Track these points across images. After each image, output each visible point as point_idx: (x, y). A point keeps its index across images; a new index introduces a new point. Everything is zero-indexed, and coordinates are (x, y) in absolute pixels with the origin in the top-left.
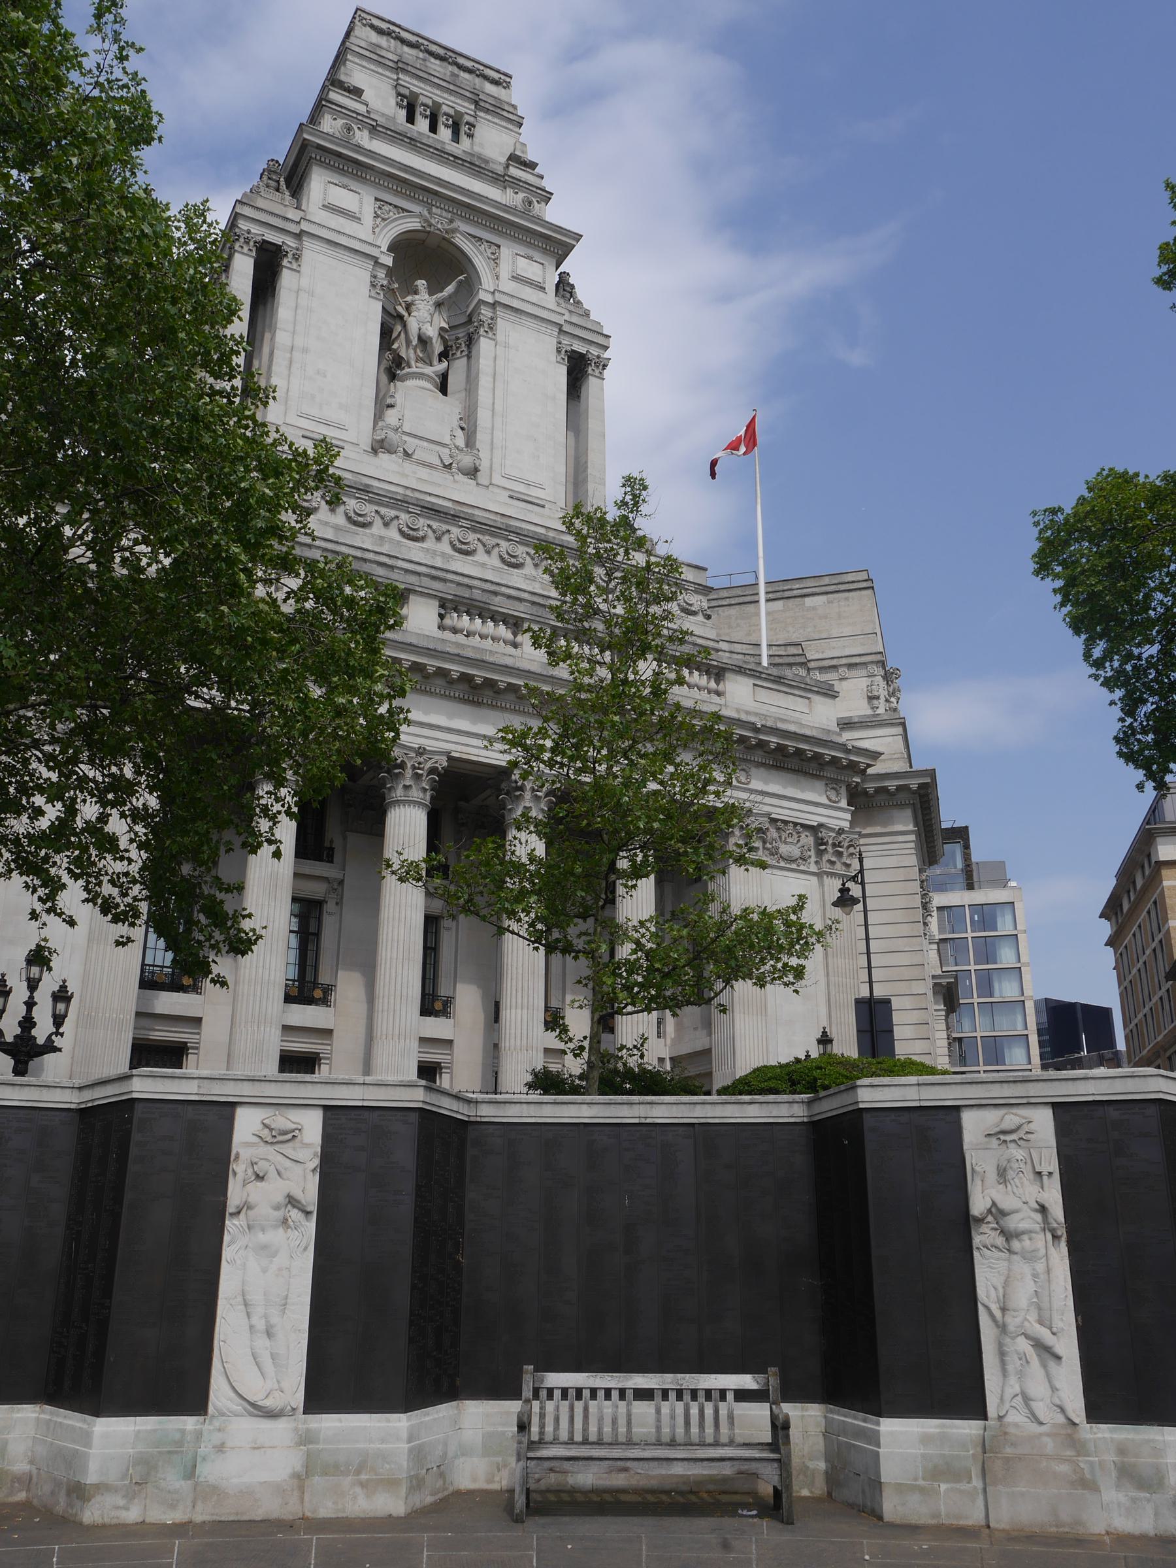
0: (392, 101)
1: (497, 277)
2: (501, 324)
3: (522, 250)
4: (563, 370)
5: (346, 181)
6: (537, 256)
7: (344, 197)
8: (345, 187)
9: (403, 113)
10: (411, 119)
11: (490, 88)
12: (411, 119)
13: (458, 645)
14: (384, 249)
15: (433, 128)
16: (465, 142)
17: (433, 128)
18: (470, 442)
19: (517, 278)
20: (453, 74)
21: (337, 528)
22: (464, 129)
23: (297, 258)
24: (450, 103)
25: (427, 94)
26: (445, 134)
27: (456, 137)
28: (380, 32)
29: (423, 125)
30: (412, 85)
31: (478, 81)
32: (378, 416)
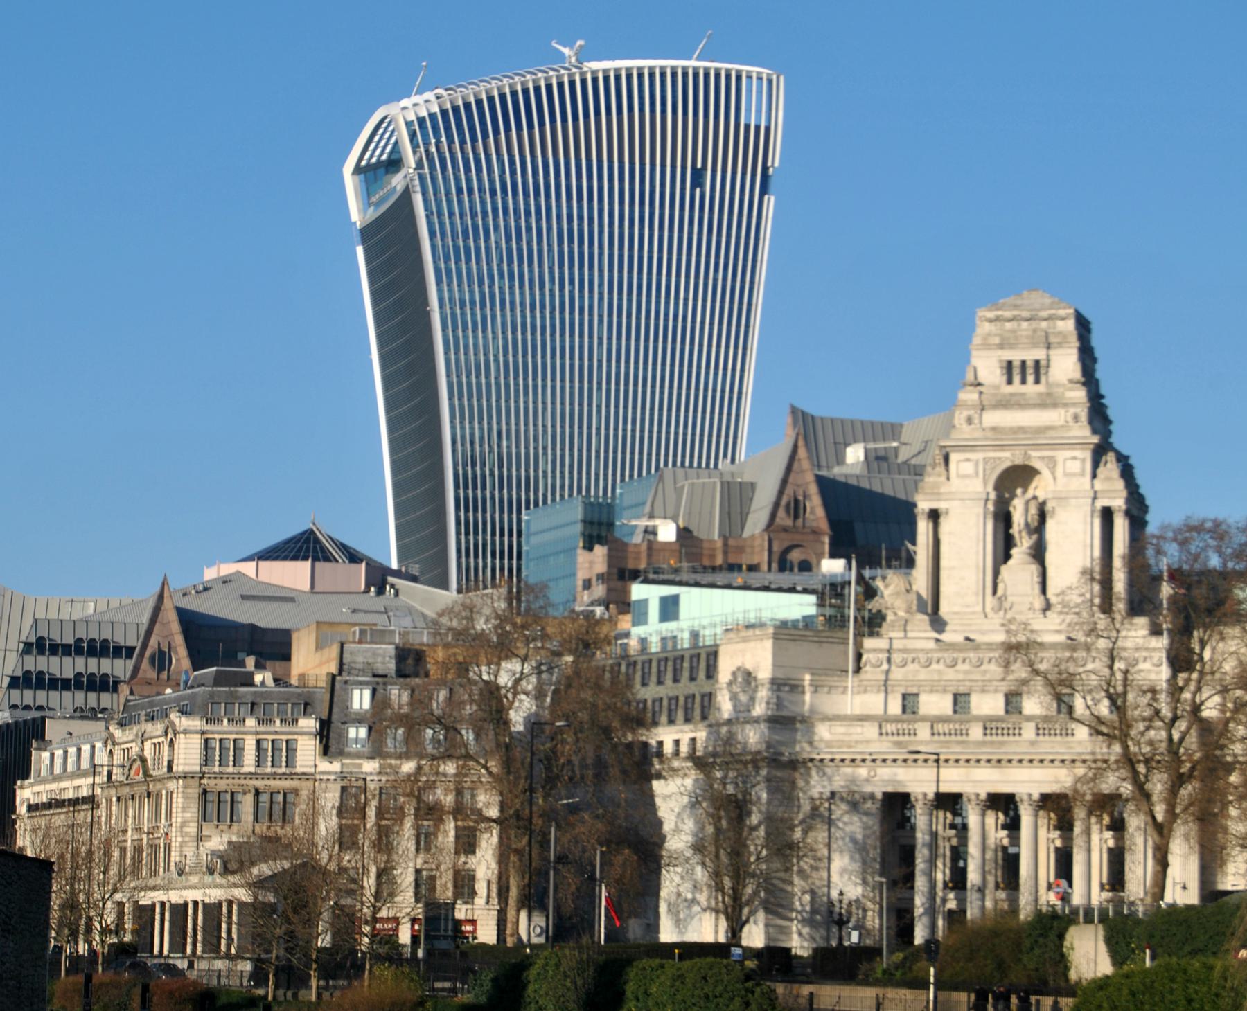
0: (998, 371)
1: (1055, 479)
2: (1058, 510)
3: (1069, 454)
4: (1097, 522)
5: (968, 455)
6: (1078, 453)
7: (968, 468)
8: (968, 460)
9: (1005, 378)
10: (1010, 382)
11: (1060, 324)
12: (1010, 382)
13: (992, 743)
14: (990, 488)
15: (1023, 382)
16: (1043, 379)
17: (1023, 382)
18: (1044, 591)
19: (1066, 474)
20: (1035, 331)
21: (966, 672)
22: (1042, 371)
23: (947, 513)
24: (1030, 356)
25: (1016, 356)
26: (1030, 378)
27: (1037, 381)
28: (990, 321)
29: (1017, 378)
30: (1008, 355)
31: (1051, 322)
32: (995, 592)
